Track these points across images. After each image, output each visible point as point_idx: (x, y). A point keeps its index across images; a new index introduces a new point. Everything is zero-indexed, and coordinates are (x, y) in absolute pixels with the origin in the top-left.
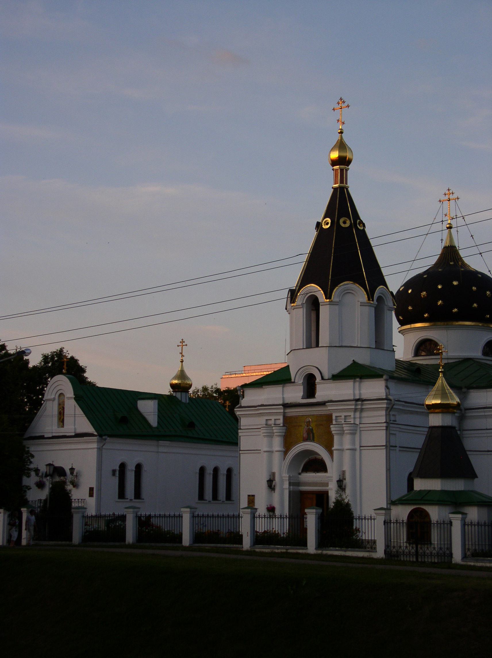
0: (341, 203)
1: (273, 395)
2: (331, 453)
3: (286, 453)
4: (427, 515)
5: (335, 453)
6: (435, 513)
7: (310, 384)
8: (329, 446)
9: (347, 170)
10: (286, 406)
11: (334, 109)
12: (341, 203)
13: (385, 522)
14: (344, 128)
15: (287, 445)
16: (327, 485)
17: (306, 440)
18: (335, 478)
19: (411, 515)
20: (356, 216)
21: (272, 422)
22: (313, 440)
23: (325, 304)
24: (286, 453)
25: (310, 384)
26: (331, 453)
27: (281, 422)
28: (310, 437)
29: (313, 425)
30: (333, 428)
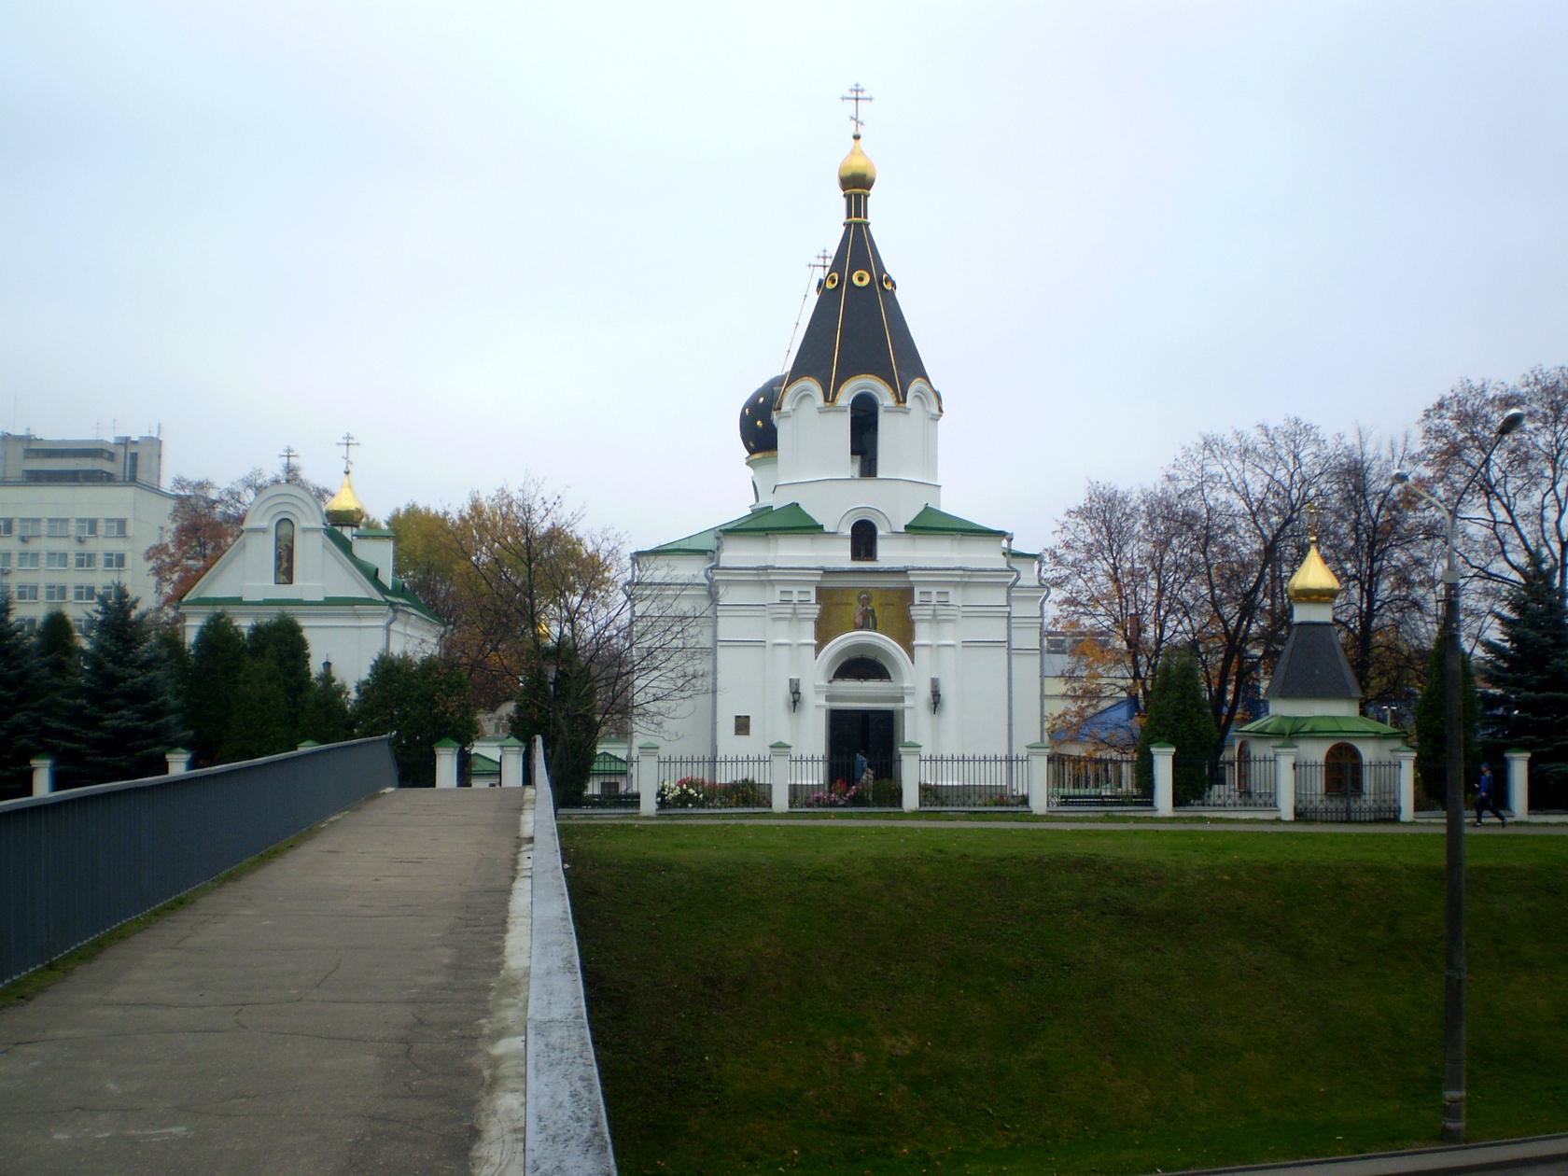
0: (857, 247)
1: (790, 553)
2: (910, 650)
3: (818, 648)
4: (1356, 755)
5: (917, 652)
6: (1368, 752)
7: (864, 538)
8: (906, 637)
9: (866, 197)
10: (827, 572)
11: (857, 95)
12: (857, 247)
13: (1294, 766)
14: (861, 131)
15: (823, 636)
16: (902, 699)
17: (861, 628)
18: (925, 693)
19: (1331, 754)
20: (881, 269)
21: (795, 598)
22: (875, 628)
23: (888, 410)
24: (818, 648)
25: (864, 538)
26: (910, 650)
27: (813, 598)
28: (868, 622)
29: (874, 605)
30: (915, 612)
